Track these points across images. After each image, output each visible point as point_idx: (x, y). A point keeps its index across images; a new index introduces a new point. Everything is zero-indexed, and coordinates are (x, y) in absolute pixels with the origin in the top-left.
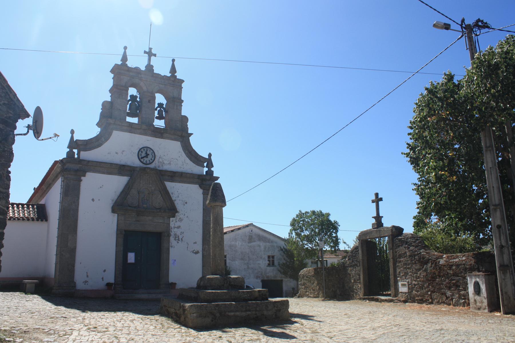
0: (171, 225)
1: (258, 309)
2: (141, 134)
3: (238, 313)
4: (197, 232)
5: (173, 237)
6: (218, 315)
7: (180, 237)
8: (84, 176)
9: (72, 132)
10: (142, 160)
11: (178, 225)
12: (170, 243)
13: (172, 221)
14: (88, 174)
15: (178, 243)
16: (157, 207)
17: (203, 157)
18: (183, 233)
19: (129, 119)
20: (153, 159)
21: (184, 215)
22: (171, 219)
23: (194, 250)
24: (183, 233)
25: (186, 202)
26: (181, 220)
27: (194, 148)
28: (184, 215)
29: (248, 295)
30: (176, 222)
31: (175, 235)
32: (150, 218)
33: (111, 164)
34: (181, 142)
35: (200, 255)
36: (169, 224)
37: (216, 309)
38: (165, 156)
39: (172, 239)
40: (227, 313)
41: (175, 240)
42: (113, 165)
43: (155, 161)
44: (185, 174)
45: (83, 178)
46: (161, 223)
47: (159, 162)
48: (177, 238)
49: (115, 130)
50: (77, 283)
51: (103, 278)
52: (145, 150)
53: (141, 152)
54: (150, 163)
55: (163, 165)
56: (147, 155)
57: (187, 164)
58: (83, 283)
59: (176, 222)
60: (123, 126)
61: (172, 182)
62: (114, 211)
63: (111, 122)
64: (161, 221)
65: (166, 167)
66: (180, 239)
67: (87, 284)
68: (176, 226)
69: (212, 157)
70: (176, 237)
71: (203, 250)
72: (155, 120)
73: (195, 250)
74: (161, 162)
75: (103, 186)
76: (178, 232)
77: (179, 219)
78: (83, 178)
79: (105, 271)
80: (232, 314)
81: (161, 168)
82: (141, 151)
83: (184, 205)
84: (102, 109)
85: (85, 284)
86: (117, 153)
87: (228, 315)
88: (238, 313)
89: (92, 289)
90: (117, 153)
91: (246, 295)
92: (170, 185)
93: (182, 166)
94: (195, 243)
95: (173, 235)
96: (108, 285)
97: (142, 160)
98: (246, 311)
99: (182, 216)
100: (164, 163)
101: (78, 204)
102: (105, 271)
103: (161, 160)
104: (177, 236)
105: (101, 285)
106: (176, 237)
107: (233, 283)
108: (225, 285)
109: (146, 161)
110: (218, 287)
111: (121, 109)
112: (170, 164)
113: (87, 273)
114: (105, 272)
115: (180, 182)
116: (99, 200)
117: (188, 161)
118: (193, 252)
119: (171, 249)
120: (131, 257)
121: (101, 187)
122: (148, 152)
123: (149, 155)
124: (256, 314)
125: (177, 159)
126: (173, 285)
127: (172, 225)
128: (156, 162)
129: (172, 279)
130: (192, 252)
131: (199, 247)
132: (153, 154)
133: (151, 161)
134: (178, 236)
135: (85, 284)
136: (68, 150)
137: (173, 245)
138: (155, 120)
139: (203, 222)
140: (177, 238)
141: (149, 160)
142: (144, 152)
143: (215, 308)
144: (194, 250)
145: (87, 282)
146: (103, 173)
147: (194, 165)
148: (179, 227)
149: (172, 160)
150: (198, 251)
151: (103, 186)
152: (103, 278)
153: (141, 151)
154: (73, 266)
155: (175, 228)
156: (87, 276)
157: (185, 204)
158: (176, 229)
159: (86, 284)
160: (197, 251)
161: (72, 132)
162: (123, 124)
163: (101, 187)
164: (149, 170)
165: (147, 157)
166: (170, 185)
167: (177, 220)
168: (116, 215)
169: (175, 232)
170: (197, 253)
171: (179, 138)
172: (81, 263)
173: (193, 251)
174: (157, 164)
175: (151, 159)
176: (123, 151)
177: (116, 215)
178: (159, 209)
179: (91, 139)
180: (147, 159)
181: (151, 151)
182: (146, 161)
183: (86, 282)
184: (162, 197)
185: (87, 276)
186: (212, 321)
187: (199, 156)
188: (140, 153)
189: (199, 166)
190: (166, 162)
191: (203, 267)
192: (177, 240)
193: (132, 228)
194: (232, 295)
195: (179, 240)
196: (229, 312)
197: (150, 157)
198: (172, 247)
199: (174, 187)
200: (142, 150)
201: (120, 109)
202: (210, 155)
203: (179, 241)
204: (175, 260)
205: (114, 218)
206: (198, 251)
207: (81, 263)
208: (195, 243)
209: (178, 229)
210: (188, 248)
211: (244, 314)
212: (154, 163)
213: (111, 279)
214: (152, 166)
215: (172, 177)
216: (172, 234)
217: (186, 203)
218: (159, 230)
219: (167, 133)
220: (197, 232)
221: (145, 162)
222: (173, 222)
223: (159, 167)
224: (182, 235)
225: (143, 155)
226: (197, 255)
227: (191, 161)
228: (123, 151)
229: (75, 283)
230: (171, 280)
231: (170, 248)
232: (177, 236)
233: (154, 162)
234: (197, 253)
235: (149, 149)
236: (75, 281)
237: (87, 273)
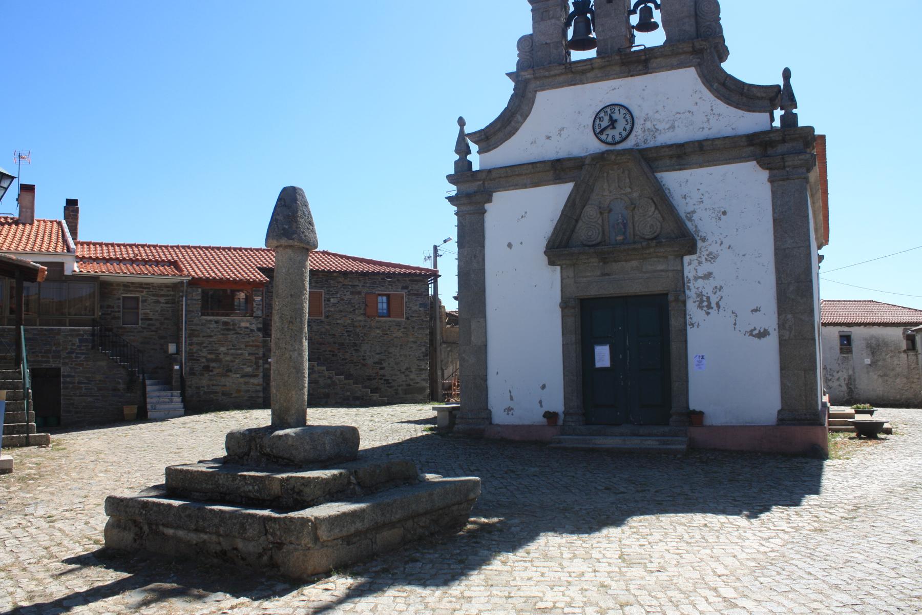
0: (686, 273)
1: (222, 530)
2: (596, 79)
3: (181, 533)
4: (759, 282)
5: (695, 302)
6: (146, 528)
7: (714, 300)
8: (489, 200)
9: (461, 122)
10: (603, 137)
11: (705, 272)
12: (688, 317)
13: (690, 264)
14: (497, 196)
15: (708, 313)
16: (647, 237)
17: (763, 87)
18: (721, 287)
19: (576, 55)
20: (628, 127)
21: (722, 243)
22: (687, 259)
23: (755, 329)
24: (721, 287)
25: (723, 210)
26: (712, 257)
27: (729, 72)
28: (722, 243)
29: (256, 487)
30: (700, 263)
31: (700, 295)
32: (634, 263)
33: (533, 164)
34: (695, 67)
35: (772, 341)
36: (682, 271)
37: (142, 513)
38: (657, 112)
39: (691, 306)
40: (161, 528)
41: (700, 307)
42: (538, 165)
43: (635, 129)
44: (710, 142)
45: (487, 206)
46: (662, 271)
47: (644, 131)
48: (705, 304)
49: (539, 91)
50: (493, 411)
51: (540, 402)
52: (609, 112)
53: (600, 120)
54: (624, 139)
55: (656, 134)
56: (613, 123)
57: (719, 115)
58: (505, 411)
59: (700, 263)
60: (555, 75)
61: (680, 169)
62: (551, 263)
63: (528, 77)
64: (660, 267)
65: (666, 138)
66: (713, 305)
67: (512, 414)
68: (700, 274)
69: (792, 81)
70: (702, 301)
71: (781, 326)
72: (635, 32)
73: (758, 329)
74: (649, 129)
75: (526, 213)
76: (707, 287)
77: (708, 255)
78: (487, 206)
79: (544, 387)
80: (170, 532)
81: (651, 144)
82: (600, 118)
83: (720, 219)
84: (519, 55)
85: (508, 414)
86: (548, 138)
87: (164, 534)
88: (181, 533)
89: (521, 424)
90: (548, 138)
91: (251, 488)
92: (673, 180)
93: (706, 125)
94: (756, 310)
95: (694, 296)
96: (550, 416)
97: (603, 137)
98: (197, 530)
99: (714, 248)
100: (657, 130)
101: (484, 260)
102: (544, 387)
103: (649, 125)
104: (705, 298)
105: (535, 416)
106: (702, 301)
107: (268, 450)
108: (252, 453)
109: (613, 137)
110: (237, 457)
111: (548, 41)
112: (673, 127)
113: (510, 392)
114: (545, 390)
115: (701, 166)
116: (521, 243)
117: (721, 107)
118: (751, 335)
119: (690, 331)
120: (603, 356)
121: (522, 217)
122: (615, 116)
123: (616, 121)
124: (219, 543)
125: (689, 112)
126: (696, 417)
127: (689, 272)
128: (638, 134)
129: (695, 404)
130: (747, 335)
131: (769, 319)
132: (628, 117)
133: (624, 134)
134: (708, 298)
135: (508, 414)
136: (457, 157)
137: (694, 321)
138: (635, 32)
139: (776, 254)
140: (705, 304)
141: (620, 134)
142: (606, 119)
143: (142, 511)
144: (755, 329)
145: (512, 409)
146: (525, 186)
147: (740, 112)
148: (708, 276)
149: (678, 116)
150: (765, 330)
151: (526, 213)
152: (540, 402)
153: (600, 118)
154: (485, 379)
155: (696, 278)
156: (512, 399)
157: (722, 217)
158: (700, 281)
159: (510, 413)
160: (762, 331)
161: (461, 122)
162: (552, 73)
163: (522, 217)
164: (613, 157)
165: (614, 128)
166: (673, 180)
167: (703, 260)
168: (558, 268)
169: (698, 288)
170: (763, 334)
171: (691, 57)
172: (497, 373)
173: (752, 331)
174: (640, 137)
175: (625, 129)
176: (562, 129)
177: (558, 268)
178: (652, 239)
179: (491, 124)
180: (614, 130)
181: (623, 111)
182: (613, 137)
183: (509, 409)
184: (657, 212)
185: (512, 399)
186: (135, 540)
187: (746, 88)
188: (598, 122)
189: (754, 111)
190: (660, 126)
191: (782, 369)
192: (705, 309)
193: (593, 291)
194: (221, 482)
195: (709, 306)
196: (164, 525)
197: (621, 125)
198: (692, 325)
199: (687, 181)
200: (602, 114)
201: (546, 43)
202: (787, 74)
203: (710, 311)
204: (703, 357)
205: (555, 274)
206: (765, 330)
207: (497, 373)
208: (756, 310)
209: (706, 281)
210: (735, 324)
211: (193, 537)
212: (632, 136)
213: (557, 404)
214: (629, 144)
215: (679, 157)
216: (691, 294)
217: (724, 213)
218: (656, 287)
219: (656, 58)
220: (759, 282)
221: (610, 140)
222: (691, 266)
223: (645, 143)
224: (718, 293)
225: (605, 123)
226: (762, 339)
227: (729, 104)
228: (562, 129)
229: (490, 412)
230: (694, 405)
231: (688, 327)
232: (705, 298)
233: (634, 133)
234: (763, 334)
235: (617, 109)
236: (489, 408)
237: (510, 392)
